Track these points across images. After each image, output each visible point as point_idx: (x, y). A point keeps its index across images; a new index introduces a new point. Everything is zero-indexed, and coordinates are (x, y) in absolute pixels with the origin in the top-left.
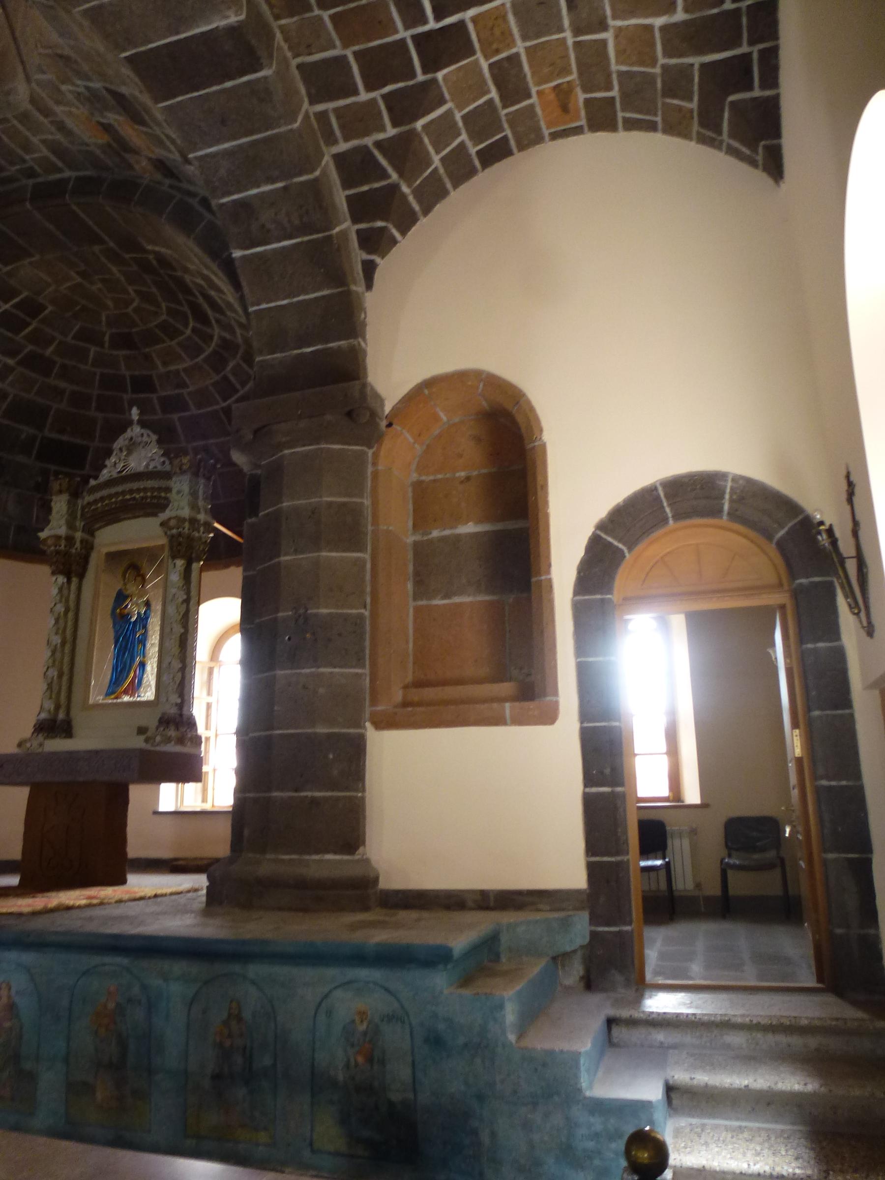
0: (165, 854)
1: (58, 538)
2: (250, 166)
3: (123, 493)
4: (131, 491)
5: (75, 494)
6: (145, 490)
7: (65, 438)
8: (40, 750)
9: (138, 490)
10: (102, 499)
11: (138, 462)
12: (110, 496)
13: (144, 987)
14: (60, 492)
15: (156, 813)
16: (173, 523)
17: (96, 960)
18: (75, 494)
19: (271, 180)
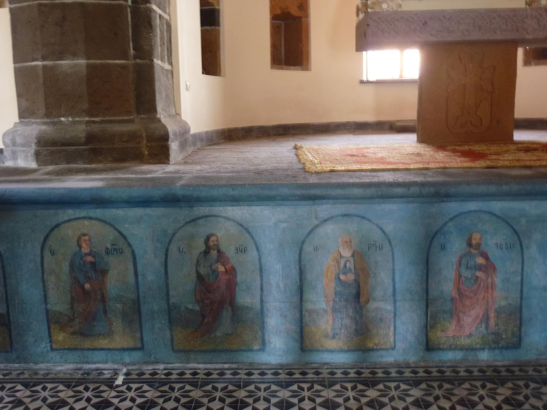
0: (370, 118)
8: (400, 10)
15: (362, 82)
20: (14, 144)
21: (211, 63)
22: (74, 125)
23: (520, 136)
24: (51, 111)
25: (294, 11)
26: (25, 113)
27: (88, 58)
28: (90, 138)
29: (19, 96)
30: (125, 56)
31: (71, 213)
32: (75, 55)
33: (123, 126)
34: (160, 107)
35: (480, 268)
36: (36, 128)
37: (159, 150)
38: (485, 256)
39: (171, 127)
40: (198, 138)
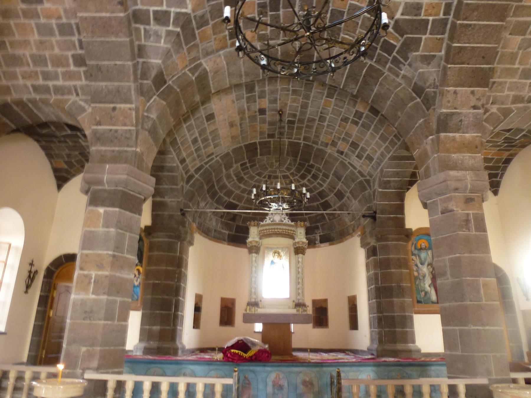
1: (257, 242)
2: (397, 174)
3: (274, 229)
4: (277, 229)
5: (258, 227)
6: (282, 229)
7: (234, 202)
9: (280, 229)
10: (266, 229)
11: (277, 218)
12: (269, 229)
13: (407, 373)
14: (254, 226)
16: (301, 243)
17: (393, 368)
18: (258, 227)
19: (399, 178)
20: (137, 348)
21: (196, 324)
22: (154, 344)
23: (294, 354)
24: (148, 340)
25: (230, 305)
26: (141, 340)
27: (161, 326)
28: (158, 348)
29: (140, 335)
30: (169, 326)
31: (153, 365)
32: (157, 326)
33: (166, 345)
34: (177, 341)
35: (248, 384)
36: (143, 345)
37: (175, 353)
38: (248, 381)
39: (180, 346)
40: (188, 350)
